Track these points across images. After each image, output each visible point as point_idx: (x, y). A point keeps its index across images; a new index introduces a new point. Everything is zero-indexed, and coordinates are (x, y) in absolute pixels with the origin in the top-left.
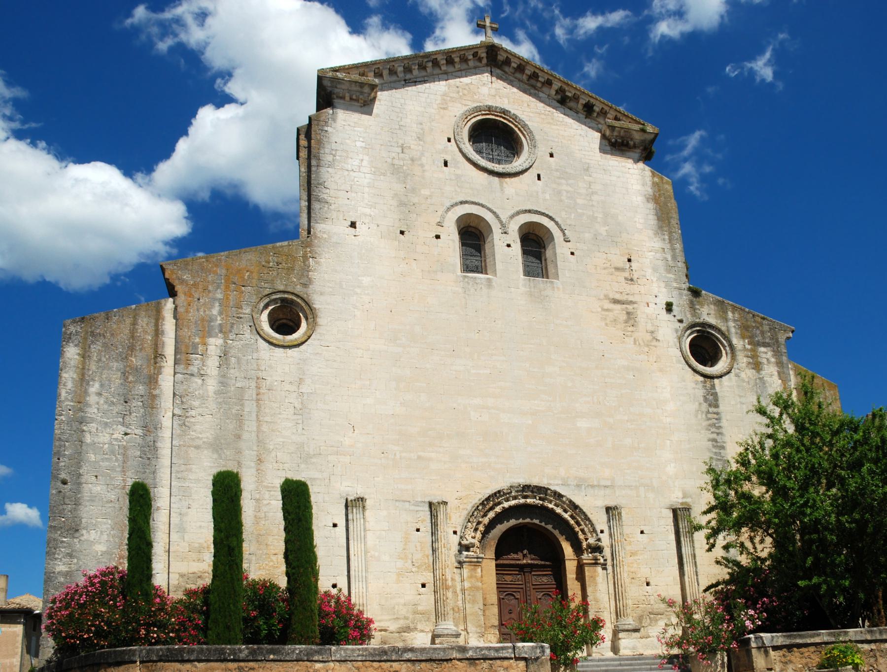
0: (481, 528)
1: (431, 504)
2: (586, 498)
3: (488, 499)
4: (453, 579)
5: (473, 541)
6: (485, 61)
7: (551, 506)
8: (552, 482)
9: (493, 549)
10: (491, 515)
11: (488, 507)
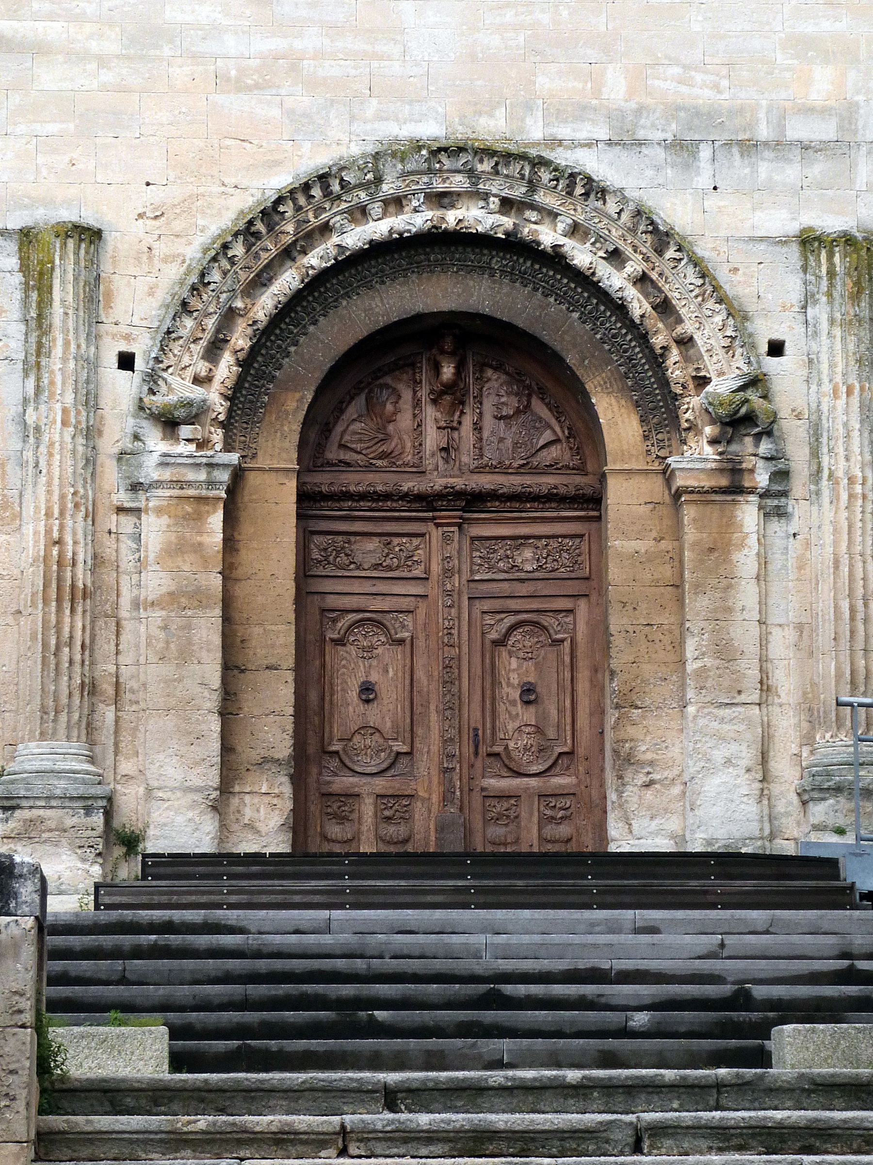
0: (240, 339)
1: (26, 237)
2: (712, 202)
3: (270, 213)
4: (97, 561)
5: (197, 393)
7: (548, 236)
8: (564, 132)
9: (293, 428)
10: (288, 281)
11: (270, 248)
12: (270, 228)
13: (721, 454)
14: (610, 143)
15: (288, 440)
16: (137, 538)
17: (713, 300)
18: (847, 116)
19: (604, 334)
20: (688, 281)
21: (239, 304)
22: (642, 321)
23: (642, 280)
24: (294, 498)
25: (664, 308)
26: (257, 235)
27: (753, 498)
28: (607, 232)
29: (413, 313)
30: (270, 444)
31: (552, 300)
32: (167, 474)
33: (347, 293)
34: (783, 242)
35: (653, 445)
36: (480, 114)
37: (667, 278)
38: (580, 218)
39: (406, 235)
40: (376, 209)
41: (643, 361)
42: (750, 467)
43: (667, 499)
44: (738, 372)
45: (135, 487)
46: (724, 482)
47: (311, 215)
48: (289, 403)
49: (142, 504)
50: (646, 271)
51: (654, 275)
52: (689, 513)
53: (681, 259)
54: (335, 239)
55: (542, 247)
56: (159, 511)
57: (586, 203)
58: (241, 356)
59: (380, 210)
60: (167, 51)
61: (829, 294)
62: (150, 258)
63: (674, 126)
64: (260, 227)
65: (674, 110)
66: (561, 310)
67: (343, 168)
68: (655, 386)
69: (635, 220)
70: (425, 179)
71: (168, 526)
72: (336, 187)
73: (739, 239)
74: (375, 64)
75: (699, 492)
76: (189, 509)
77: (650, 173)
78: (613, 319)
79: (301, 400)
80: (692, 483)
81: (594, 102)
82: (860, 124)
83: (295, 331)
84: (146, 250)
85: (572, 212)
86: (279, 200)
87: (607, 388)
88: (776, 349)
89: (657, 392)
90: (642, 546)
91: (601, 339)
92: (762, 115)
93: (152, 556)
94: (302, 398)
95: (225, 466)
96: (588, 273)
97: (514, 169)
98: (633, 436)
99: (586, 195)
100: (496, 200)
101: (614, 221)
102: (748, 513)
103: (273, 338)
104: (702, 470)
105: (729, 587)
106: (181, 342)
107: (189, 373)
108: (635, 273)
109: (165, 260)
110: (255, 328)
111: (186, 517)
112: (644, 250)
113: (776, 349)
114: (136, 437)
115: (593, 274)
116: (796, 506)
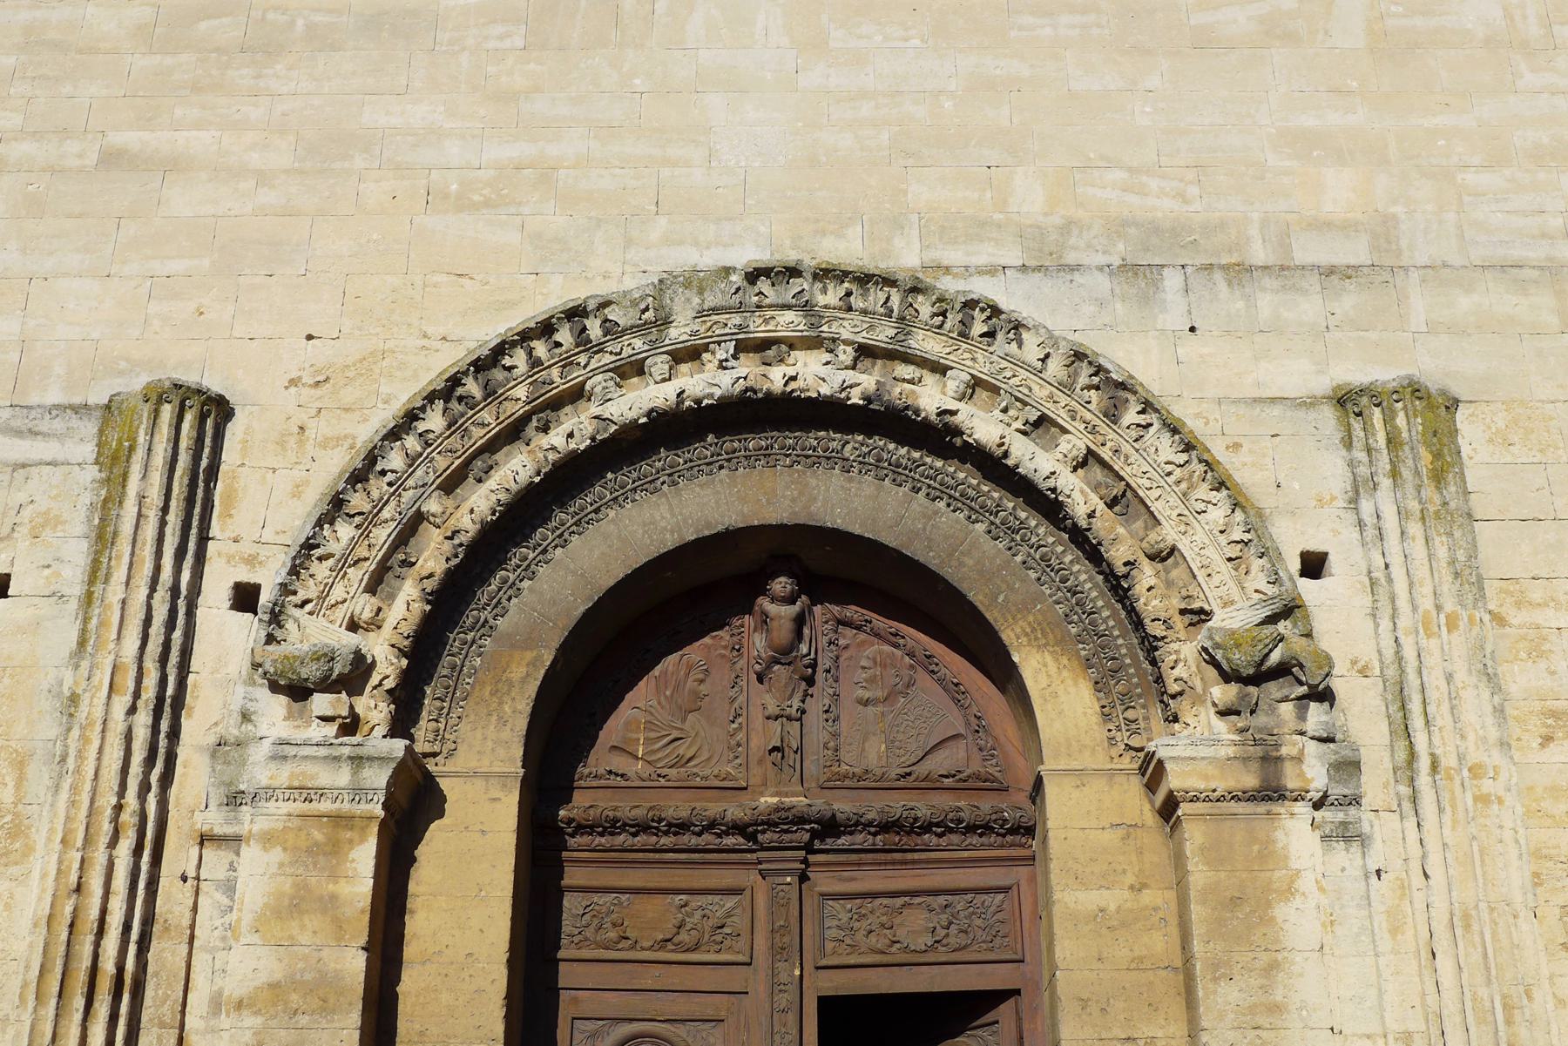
0: (433, 556)
2: (1190, 348)
7: (931, 397)
8: (953, 256)
10: (518, 468)
11: (490, 420)
13: (1242, 731)
14: (1024, 268)
15: (509, 725)
16: (230, 888)
17: (1206, 486)
18: (1384, 231)
20: (1162, 458)
21: (433, 506)
24: (512, 822)
27: (1303, 809)
28: (1026, 391)
29: (720, 528)
30: (479, 734)
32: (283, 775)
34: (1309, 403)
35: (1119, 728)
36: (824, 233)
37: (1127, 457)
38: (982, 369)
39: (705, 402)
40: (659, 365)
41: (1094, 594)
42: (1294, 752)
43: (1150, 818)
44: (1257, 596)
45: (234, 800)
46: (1250, 781)
47: (555, 372)
48: (514, 666)
49: (244, 829)
50: (1093, 447)
51: (1106, 454)
52: (1194, 834)
54: (594, 409)
56: (268, 839)
58: (430, 585)
60: (359, 162)
61: (1395, 474)
62: (301, 443)
63: (1121, 247)
65: (1119, 227)
66: (957, 521)
67: (606, 304)
68: (1116, 633)
70: (736, 319)
71: (281, 865)
73: (1236, 401)
74: (666, 172)
75: (1207, 800)
76: (318, 835)
77: (1088, 309)
79: (533, 664)
80: (1196, 783)
81: (998, 216)
82: (1404, 243)
83: (531, 556)
84: (296, 430)
85: (969, 363)
87: (1036, 639)
88: (1313, 565)
89: (1120, 641)
90: (1113, 899)
92: (1254, 231)
93: (247, 919)
94: (539, 658)
95: (382, 759)
97: (876, 297)
98: (1085, 714)
99: (990, 334)
100: (849, 349)
102: (1296, 831)
104: (1213, 760)
105: (1272, 968)
106: (331, 562)
107: (341, 613)
108: (1075, 453)
109: (325, 444)
110: (456, 541)
111: (313, 850)
112: (1089, 416)
113: (1313, 565)
114: (246, 717)
115: (1006, 454)
116: (1376, 822)
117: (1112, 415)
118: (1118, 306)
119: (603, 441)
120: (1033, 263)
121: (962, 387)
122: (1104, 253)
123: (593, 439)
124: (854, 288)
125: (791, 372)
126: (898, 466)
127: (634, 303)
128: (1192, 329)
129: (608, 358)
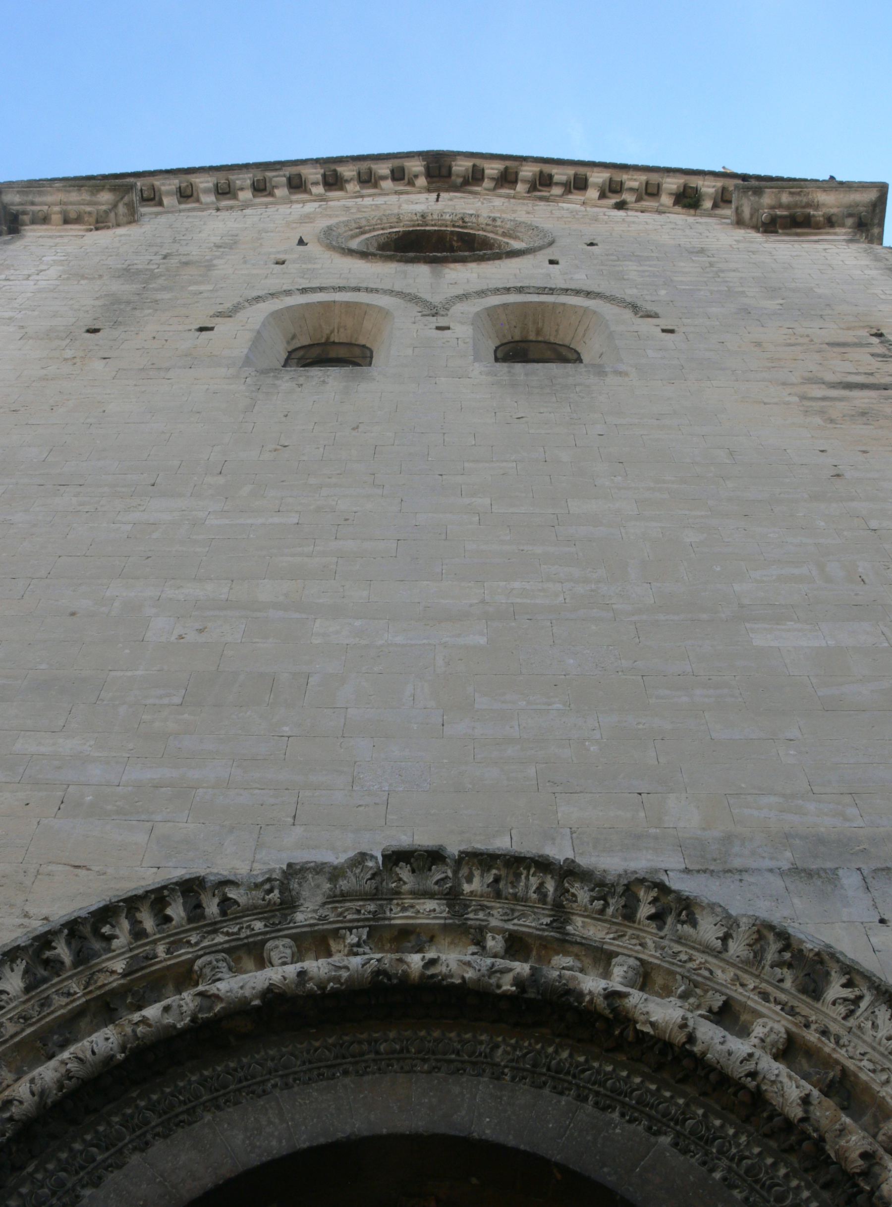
3: (86, 931)
6: (422, 181)
12: (82, 958)
19: (730, 1169)
22: (806, 1111)
23: (789, 1050)
25: (843, 1088)
26: (54, 966)
28: (707, 974)
31: (616, 1115)
33: (216, 1098)
38: (651, 955)
40: (279, 948)
47: (161, 949)
50: (794, 1029)
51: (812, 1036)
53: (860, 998)
55: (587, 998)
57: (662, 934)
59: (289, 951)
63: (788, 854)
64: (63, 951)
69: (757, 947)
70: (372, 907)
72: (212, 908)
78: (743, 1139)
81: (652, 831)
83: (99, 1158)
86: (106, 914)
91: (724, 1179)
96: (680, 1038)
99: (658, 918)
100: (499, 938)
101: (718, 954)
103: (50, 1167)
108: (773, 1036)
112: (783, 997)
115: (691, 1039)
117: (813, 989)
118: (796, 901)
119: (207, 1023)
120: (697, 867)
121: (631, 974)
122: (771, 859)
123: (194, 1019)
124: (503, 872)
125: (431, 955)
126: (557, 1072)
127: (257, 886)
128: (882, 921)
129: (220, 938)
